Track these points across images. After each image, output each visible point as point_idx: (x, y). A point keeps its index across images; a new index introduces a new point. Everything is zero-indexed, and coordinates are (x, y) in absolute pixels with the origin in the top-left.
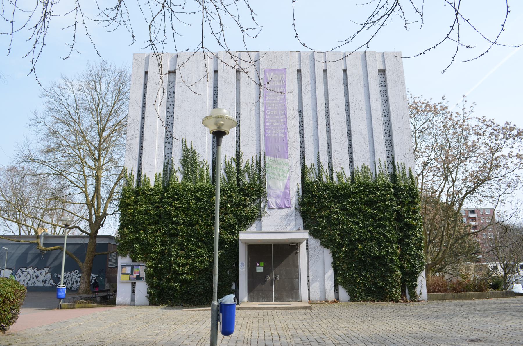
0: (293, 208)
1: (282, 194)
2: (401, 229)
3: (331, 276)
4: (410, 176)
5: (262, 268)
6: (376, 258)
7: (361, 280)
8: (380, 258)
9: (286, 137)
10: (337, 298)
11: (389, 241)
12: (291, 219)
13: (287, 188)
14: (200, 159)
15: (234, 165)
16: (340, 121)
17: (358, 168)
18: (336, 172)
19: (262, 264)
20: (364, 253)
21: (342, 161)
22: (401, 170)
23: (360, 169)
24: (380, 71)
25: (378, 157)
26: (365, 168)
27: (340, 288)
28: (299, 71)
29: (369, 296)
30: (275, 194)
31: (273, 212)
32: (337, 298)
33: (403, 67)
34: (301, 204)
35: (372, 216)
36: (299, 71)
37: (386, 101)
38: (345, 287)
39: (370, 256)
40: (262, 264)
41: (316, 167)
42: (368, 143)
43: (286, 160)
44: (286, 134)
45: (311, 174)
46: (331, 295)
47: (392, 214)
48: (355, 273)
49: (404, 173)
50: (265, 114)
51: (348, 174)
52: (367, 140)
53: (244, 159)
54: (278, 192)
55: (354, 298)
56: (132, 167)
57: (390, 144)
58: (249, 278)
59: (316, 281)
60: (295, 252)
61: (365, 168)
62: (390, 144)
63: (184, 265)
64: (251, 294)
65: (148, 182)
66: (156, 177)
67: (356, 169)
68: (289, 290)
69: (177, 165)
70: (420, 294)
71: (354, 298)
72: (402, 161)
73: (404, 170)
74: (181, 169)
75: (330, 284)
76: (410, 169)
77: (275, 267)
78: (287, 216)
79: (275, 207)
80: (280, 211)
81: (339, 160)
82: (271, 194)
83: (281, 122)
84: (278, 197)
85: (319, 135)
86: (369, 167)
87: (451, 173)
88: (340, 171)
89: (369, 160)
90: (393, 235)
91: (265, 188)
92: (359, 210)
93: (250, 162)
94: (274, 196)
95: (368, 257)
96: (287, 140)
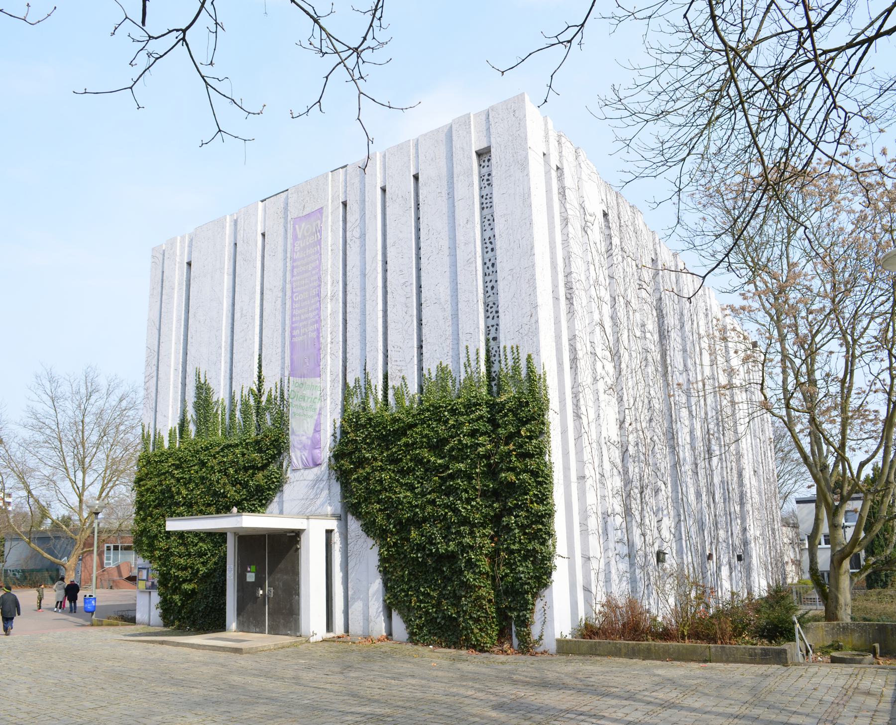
0: (324, 466)
1: (309, 442)
2: (495, 495)
3: (377, 591)
4: (528, 374)
5: (253, 574)
6: (441, 558)
7: (421, 601)
8: (451, 557)
9: (318, 337)
10: (390, 634)
11: (465, 521)
12: (321, 486)
13: (317, 430)
14: (214, 399)
15: (252, 402)
16: (404, 283)
17: (430, 373)
18: (393, 388)
19: (253, 568)
20: (421, 548)
21: (403, 363)
22: (510, 363)
23: (433, 375)
24: (479, 154)
25: (465, 343)
26: (442, 369)
27: (395, 614)
28: (345, 204)
29: (435, 635)
30: (301, 442)
31: (298, 474)
32: (390, 634)
33: (525, 129)
34: (338, 456)
35: (438, 469)
36: (345, 204)
37: (488, 221)
38: (400, 613)
39: (431, 554)
40: (253, 568)
41: (362, 383)
42: (450, 318)
43: (318, 379)
44: (318, 331)
45: (355, 398)
46: (379, 626)
47: (474, 465)
48: (411, 587)
49: (516, 368)
50: (293, 301)
51: (413, 388)
52: (449, 312)
53: (266, 387)
54: (304, 438)
55: (414, 638)
56: (148, 420)
57: (492, 310)
58: (238, 591)
59: (359, 598)
60: (294, 548)
61: (442, 369)
62: (492, 310)
63: (185, 568)
64: (241, 618)
65: (162, 442)
66: (170, 434)
67: (427, 376)
68: (286, 614)
69: (191, 413)
70: (541, 638)
71: (414, 638)
72: (514, 343)
73: (516, 360)
74: (194, 417)
75: (376, 606)
76: (529, 356)
77: (270, 574)
78: (318, 480)
79: (301, 466)
80: (307, 471)
81: (398, 363)
82: (296, 444)
83: (312, 311)
84: (304, 447)
85: (367, 321)
86: (450, 368)
87: (873, 313)
88: (399, 385)
89: (450, 353)
90: (477, 509)
91: (288, 434)
92: (419, 461)
93: (273, 393)
94: (300, 447)
95: (428, 556)
96: (319, 341)
